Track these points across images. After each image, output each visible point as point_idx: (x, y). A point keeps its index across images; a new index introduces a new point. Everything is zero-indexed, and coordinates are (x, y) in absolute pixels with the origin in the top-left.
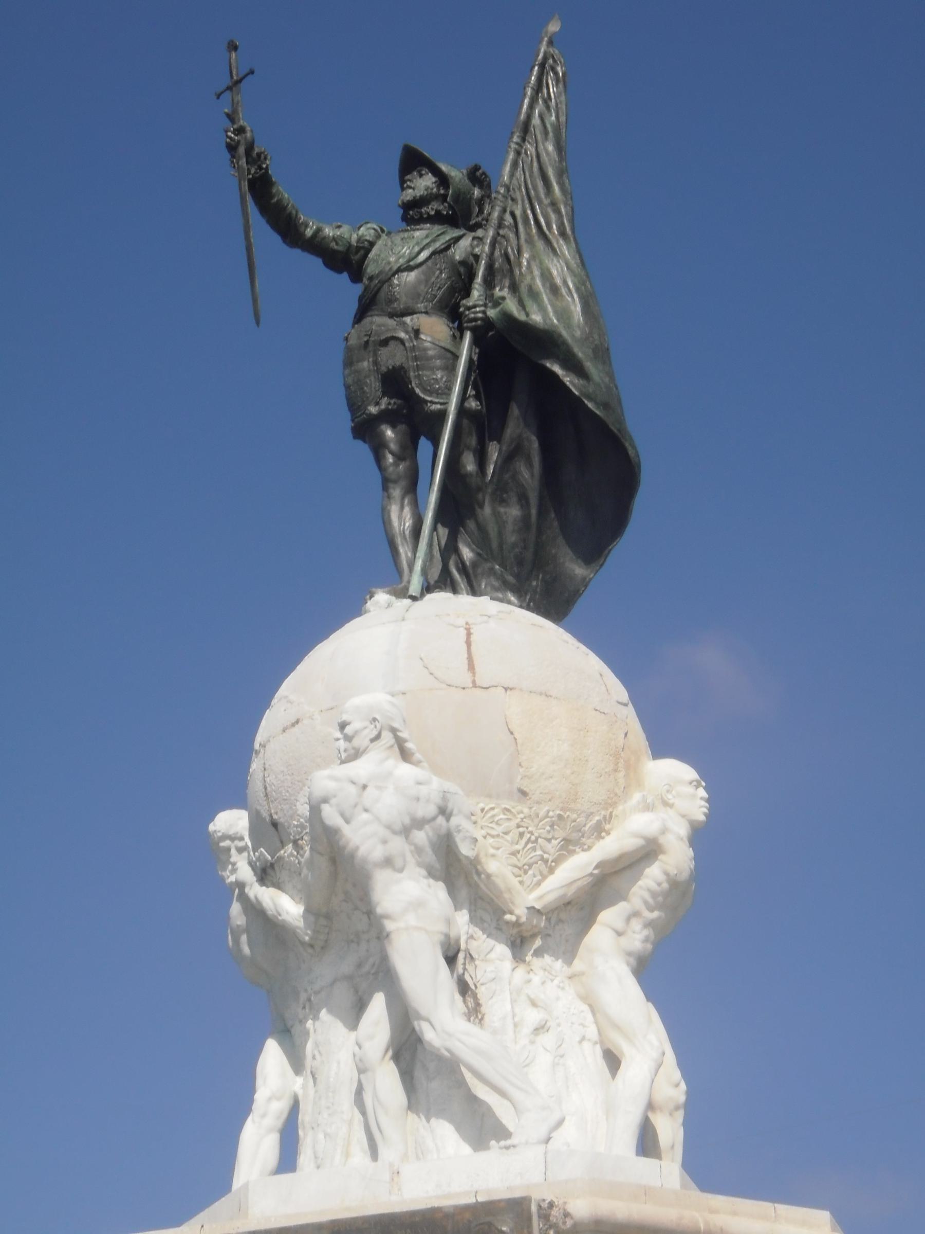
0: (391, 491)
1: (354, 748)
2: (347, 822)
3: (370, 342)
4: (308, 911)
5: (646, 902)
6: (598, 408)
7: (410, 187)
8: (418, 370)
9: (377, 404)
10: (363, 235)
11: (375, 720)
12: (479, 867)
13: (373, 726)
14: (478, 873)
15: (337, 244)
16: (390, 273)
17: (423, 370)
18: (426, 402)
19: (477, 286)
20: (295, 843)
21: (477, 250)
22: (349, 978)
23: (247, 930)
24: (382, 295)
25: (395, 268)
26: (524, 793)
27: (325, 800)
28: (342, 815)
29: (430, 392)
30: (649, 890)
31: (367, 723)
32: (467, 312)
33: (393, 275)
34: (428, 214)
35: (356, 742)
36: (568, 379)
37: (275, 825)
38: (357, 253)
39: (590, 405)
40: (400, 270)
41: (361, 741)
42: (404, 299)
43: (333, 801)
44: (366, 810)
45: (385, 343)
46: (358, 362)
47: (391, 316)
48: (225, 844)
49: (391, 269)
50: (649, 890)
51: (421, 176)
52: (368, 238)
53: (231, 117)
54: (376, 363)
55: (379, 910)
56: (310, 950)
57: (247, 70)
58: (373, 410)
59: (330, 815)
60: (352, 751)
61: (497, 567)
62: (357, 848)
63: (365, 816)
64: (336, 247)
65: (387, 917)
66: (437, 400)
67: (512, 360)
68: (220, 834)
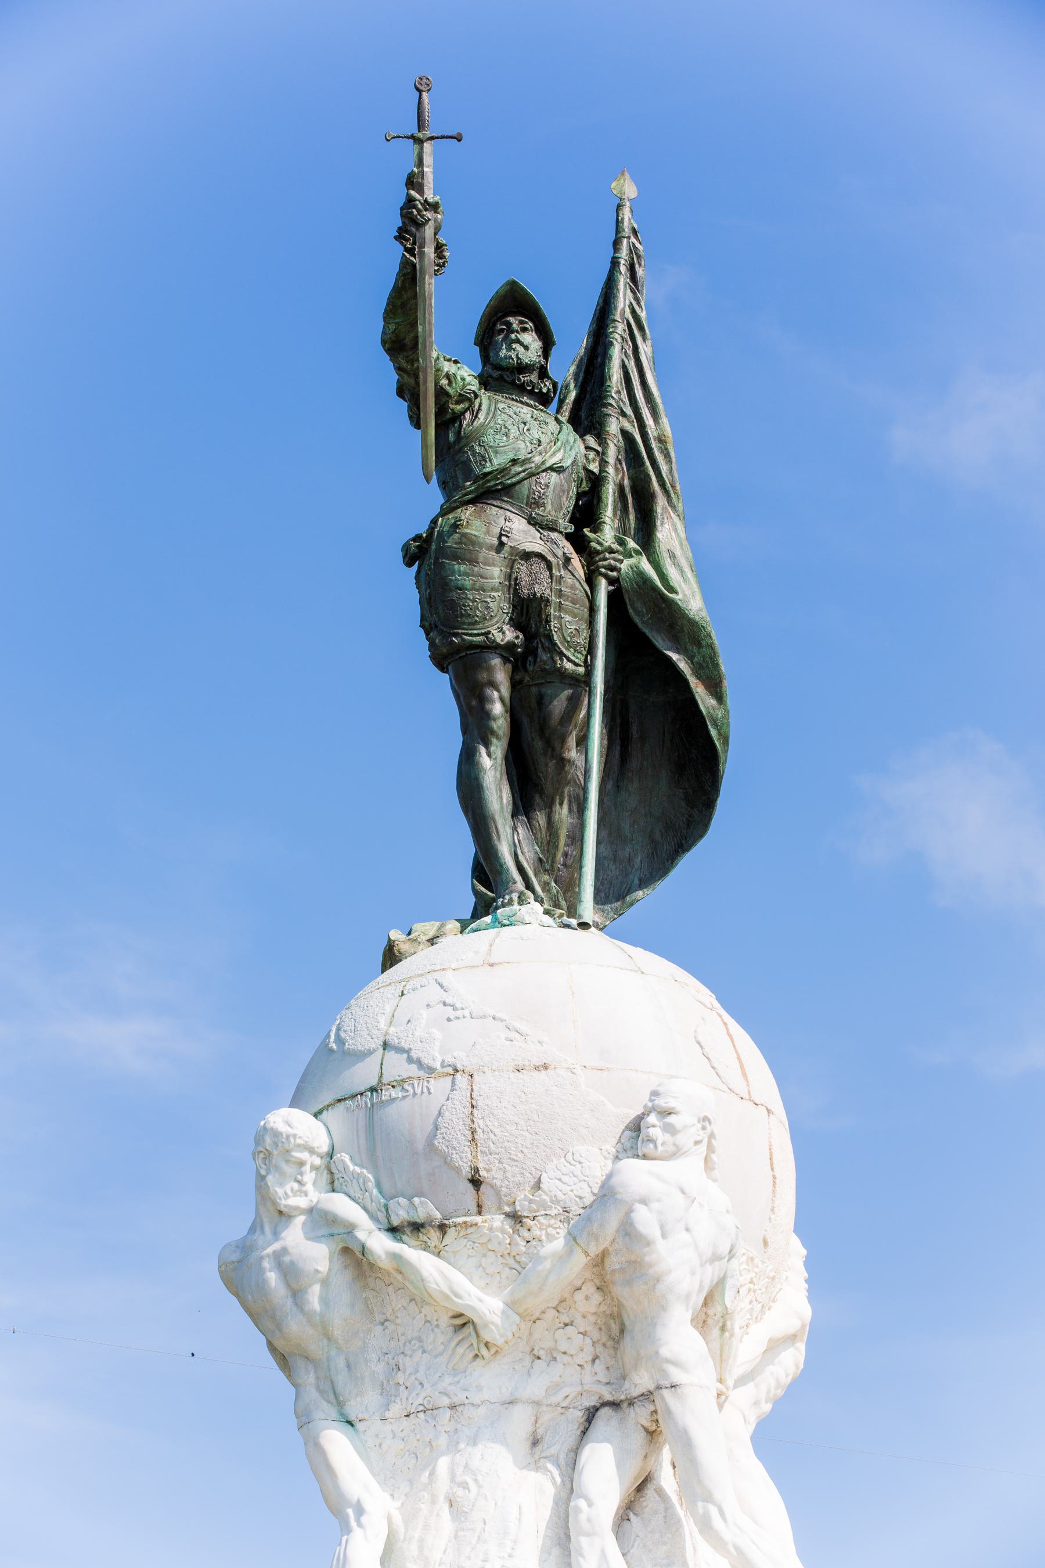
0: (493, 749)
1: (675, 1145)
2: (664, 1236)
3: (506, 549)
4: (512, 1305)
5: (768, 1392)
6: (719, 740)
7: (522, 344)
8: (560, 611)
9: (501, 631)
10: (469, 384)
11: (706, 1119)
12: (729, 1323)
13: (700, 1126)
14: (723, 1329)
15: (450, 384)
16: (544, 467)
17: (566, 612)
18: (562, 654)
19: (607, 520)
20: (515, 1218)
21: (594, 467)
22: (537, 1403)
23: (325, 1282)
24: (524, 489)
25: (548, 465)
26: (765, 1243)
27: (644, 1202)
28: (662, 1227)
29: (569, 645)
30: (777, 1380)
31: (695, 1121)
32: (607, 555)
33: (543, 471)
34: (541, 389)
35: (680, 1139)
36: (699, 690)
37: (476, 1182)
38: (458, 403)
39: (713, 732)
40: (551, 468)
41: (685, 1140)
42: (549, 507)
43: (655, 1206)
44: (687, 1230)
45: (527, 556)
46: (485, 564)
47: (532, 521)
48: (304, 1156)
49: (543, 463)
50: (777, 1380)
51: (524, 330)
52: (473, 388)
53: (414, 182)
54: (509, 577)
55: (664, 1352)
56: (484, 1351)
57: (454, 133)
58: (498, 638)
59: (645, 1219)
60: (672, 1149)
61: (553, 884)
62: (670, 1271)
63: (685, 1236)
64: (448, 388)
65: (675, 1364)
66: (573, 658)
67: (647, 638)
68: (299, 1141)
